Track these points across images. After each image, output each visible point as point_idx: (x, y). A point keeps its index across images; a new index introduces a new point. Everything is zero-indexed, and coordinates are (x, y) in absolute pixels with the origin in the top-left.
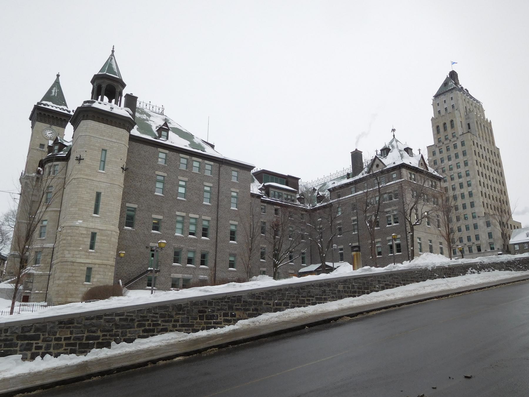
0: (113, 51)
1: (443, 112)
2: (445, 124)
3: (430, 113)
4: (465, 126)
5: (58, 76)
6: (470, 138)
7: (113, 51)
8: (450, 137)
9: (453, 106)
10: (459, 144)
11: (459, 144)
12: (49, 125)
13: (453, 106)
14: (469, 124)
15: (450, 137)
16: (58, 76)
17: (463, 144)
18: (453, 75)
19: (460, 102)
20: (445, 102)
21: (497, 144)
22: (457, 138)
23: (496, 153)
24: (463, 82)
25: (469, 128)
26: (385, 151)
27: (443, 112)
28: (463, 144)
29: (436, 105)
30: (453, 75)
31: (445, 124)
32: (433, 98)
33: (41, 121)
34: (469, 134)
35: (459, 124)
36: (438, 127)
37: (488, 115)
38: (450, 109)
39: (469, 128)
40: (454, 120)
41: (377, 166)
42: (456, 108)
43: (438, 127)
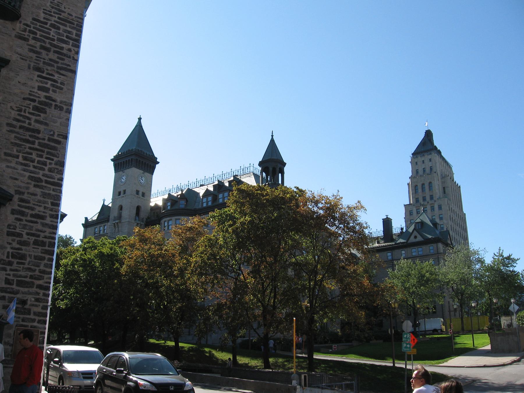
0: (272, 136)
1: (421, 172)
2: (423, 184)
3: (409, 172)
4: (441, 190)
5: (140, 119)
6: (446, 203)
7: (272, 136)
8: (428, 198)
9: (431, 169)
10: (436, 207)
11: (436, 207)
12: (142, 172)
13: (431, 169)
14: (444, 188)
15: (428, 198)
16: (140, 119)
17: (440, 207)
18: (429, 134)
19: (438, 164)
20: (423, 162)
21: (465, 211)
22: (435, 201)
23: (463, 218)
24: (437, 143)
25: (444, 192)
26: (420, 224)
27: (421, 172)
28: (440, 207)
29: (414, 163)
30: (429, 134)
31: (423, 184)
32: (411, 156)
33: (136, 167)
34: (446, 199)
35: (437, 187)
36: (416, 186)
37: (457, 179)
38: (428, 170)
39: (444, 192)
40: (433, 182)
41: (415, 237)
42: (434, 170)
43: (416, 186)
